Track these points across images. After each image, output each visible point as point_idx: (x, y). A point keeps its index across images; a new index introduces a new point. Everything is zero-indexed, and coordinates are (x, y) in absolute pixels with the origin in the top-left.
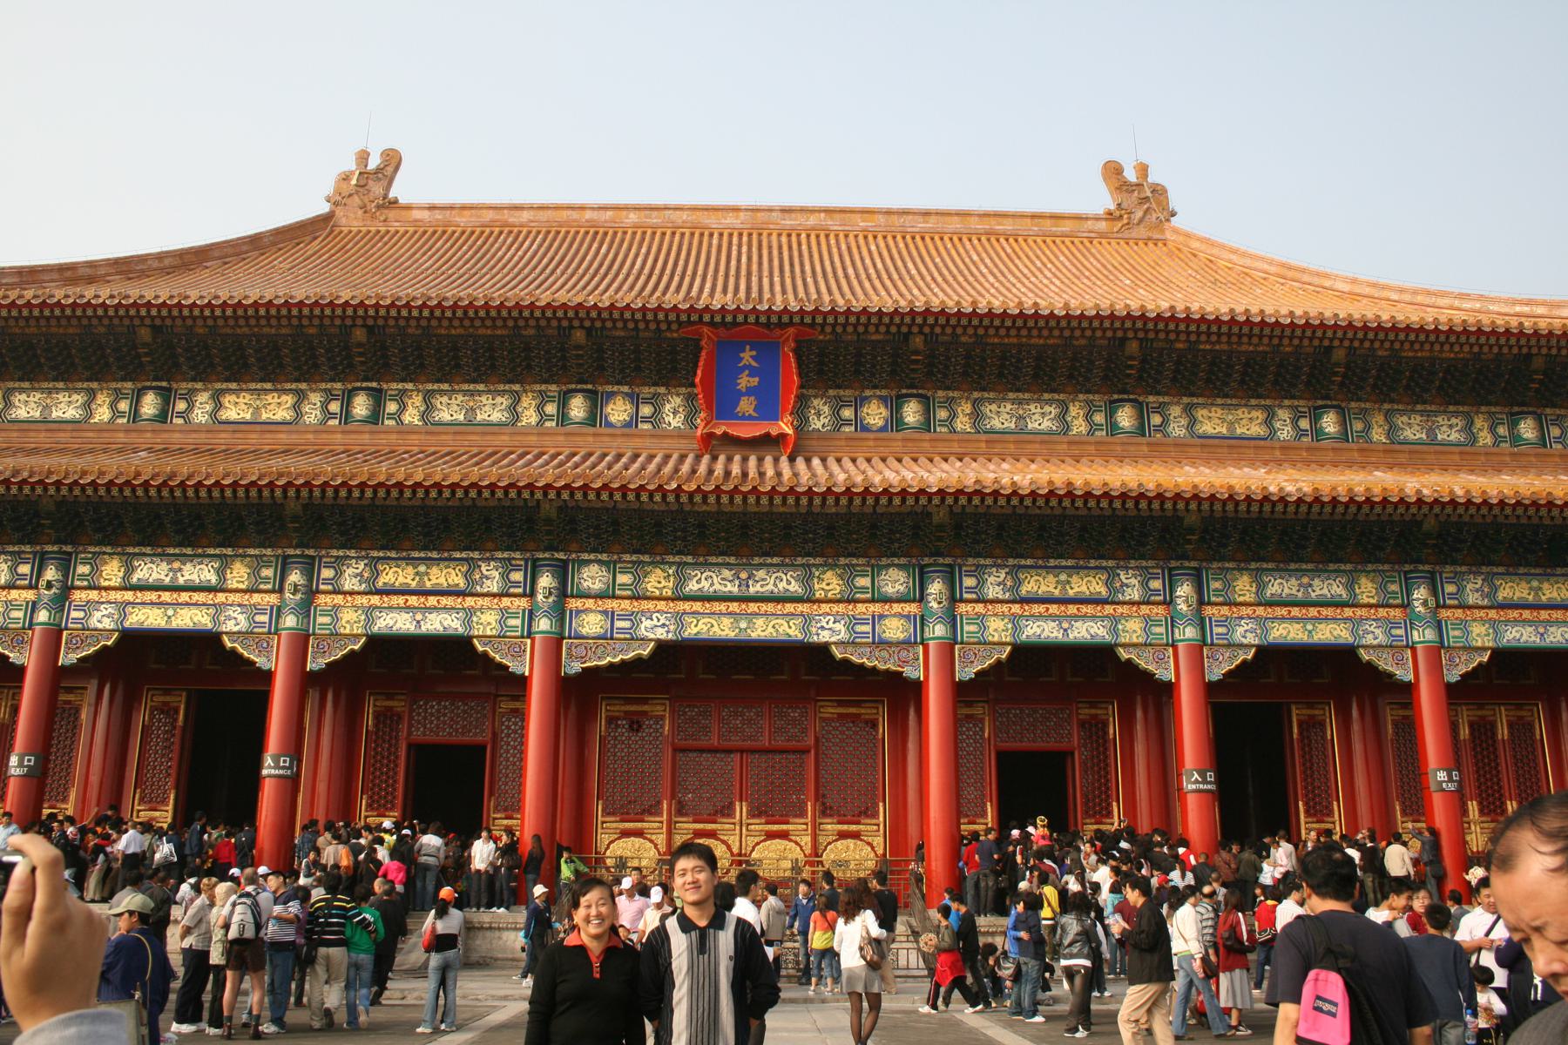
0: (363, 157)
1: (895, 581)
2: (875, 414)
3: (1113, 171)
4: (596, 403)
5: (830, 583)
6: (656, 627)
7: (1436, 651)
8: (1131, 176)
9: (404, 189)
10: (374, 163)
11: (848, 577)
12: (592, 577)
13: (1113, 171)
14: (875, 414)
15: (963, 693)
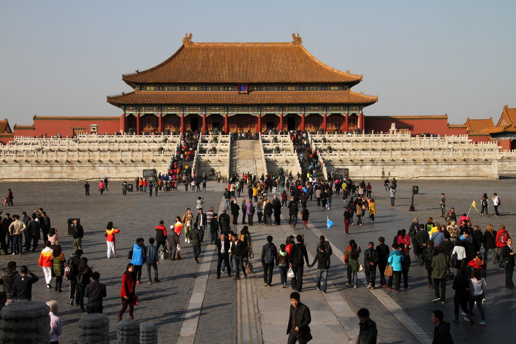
0: (187, 35)
1: (256, 108)
2: (255, 89)
3: (294, 35)
4: (228, 88)
5: (250, 109)
6: (235, 113)
7: (304, 114)
8: (296, 36)
9: (193, 40)
10: (188, 36)
11: (252, 108)
12: (230, 108)
13: (294, 35)
14: (255, 89)
15: (261, 118)
